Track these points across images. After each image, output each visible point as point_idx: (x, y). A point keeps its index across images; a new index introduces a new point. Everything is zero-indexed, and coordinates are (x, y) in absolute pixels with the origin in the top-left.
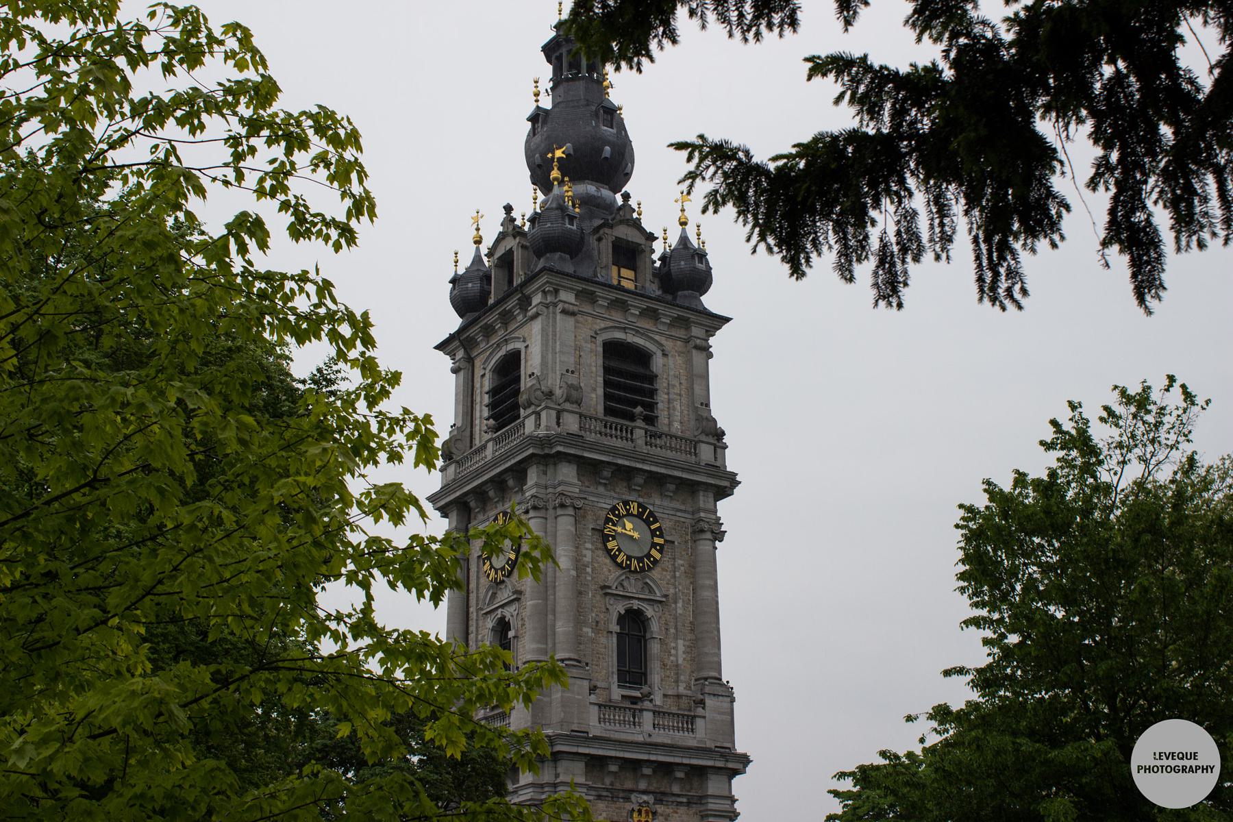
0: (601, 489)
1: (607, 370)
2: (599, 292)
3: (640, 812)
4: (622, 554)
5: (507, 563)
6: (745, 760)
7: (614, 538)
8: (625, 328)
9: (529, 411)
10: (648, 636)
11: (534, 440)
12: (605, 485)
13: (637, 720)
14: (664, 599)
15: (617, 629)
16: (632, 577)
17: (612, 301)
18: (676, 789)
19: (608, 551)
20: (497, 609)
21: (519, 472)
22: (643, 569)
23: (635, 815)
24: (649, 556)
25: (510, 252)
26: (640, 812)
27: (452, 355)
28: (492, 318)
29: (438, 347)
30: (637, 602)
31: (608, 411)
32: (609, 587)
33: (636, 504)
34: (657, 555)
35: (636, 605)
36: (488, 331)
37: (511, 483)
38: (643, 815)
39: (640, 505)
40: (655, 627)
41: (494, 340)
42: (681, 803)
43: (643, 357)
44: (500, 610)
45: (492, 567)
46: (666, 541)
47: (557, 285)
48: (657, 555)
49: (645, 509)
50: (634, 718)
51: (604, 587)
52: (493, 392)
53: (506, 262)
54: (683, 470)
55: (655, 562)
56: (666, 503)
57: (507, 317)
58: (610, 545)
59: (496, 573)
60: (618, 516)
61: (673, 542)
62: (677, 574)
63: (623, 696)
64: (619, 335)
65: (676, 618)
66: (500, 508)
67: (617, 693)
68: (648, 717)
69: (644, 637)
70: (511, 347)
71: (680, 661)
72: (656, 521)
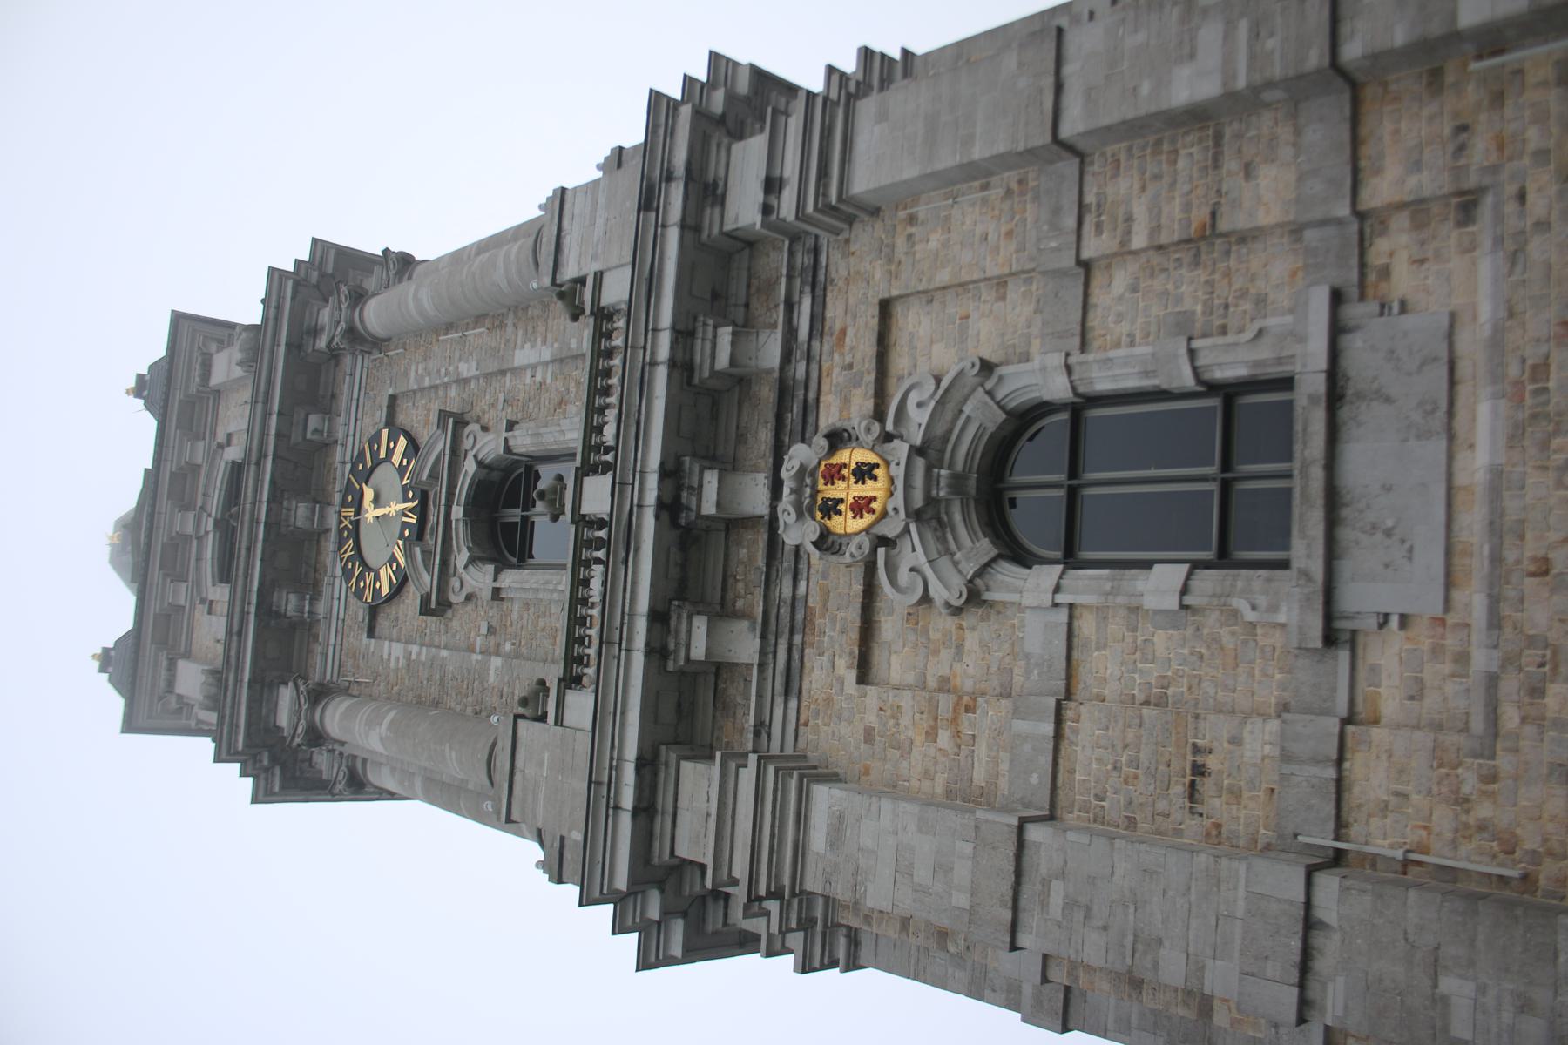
0: (321, 608)
3: (831, 508)
7: (377, 578)
12: (314, 600)
17: (166, 575)
18: (769, 351)
23: (837, 524)
26: (831, 508)
30: (455, 508)
35: (457, 512)
38: (838, 490)
39: (344, 504)
42: (817, 319)
54: (267, 414)
56: (340, 435)
58: (385, 590)
61: (393, 400)
62: (427, 383)
65: (488, 376)
71: (546, 355)
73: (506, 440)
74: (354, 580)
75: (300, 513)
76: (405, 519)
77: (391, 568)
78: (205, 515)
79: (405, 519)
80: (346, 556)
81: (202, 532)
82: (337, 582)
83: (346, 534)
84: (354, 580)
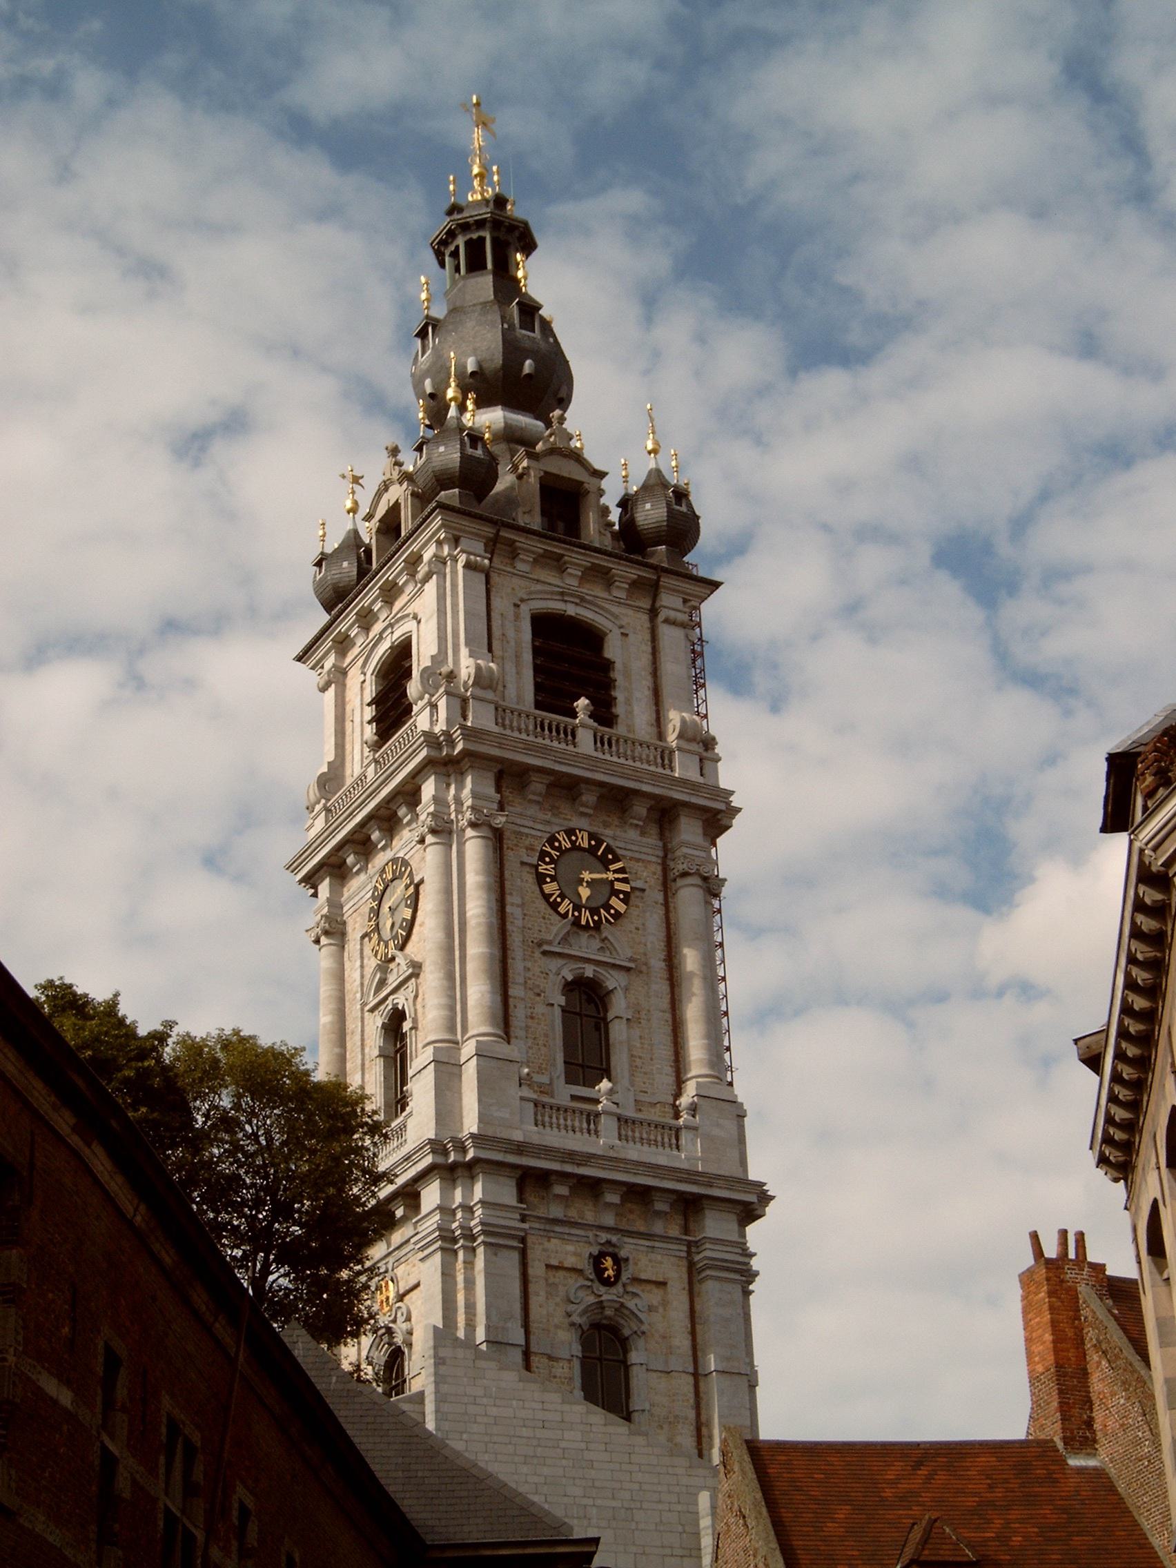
1: (536, 651)
2: (521, 540)
4: (567, 901)
5: (401, 927)
6: (765, 1198)
7: (553, 878)
8: (562, 594)
9: (421, 704)
10: (610, 1016)
11: (430, 739)
13: (592, 1126)
14: (632, 965)
15: (562, 1000)
16: (584, 936)
19: (546, 897)
20: (386, 998)
21: (409, 794)
22: (598, 924)
24: (608, 907)
25: (395, 509)
27: (317, 666)
28: (370, 597)
29: (300, 659)
31: (538, 705)
32: (550, 943)
33: (586, 835)
34: (621, 907)
35: (589, 971)
36: (366, 619)
37: (402, 811)
39: (592, 836)
40: (619, 1006)
41: (377, 628)
43: (592, 638)
44: (391, 998)
45: (380, 939)
46: (631, 888)
47: (460, 530)
48: (621, 907)
49: (600, 842)
50: (589, 1124)
51: (540, 945)
52: (377, 701)
53: (390, 527)
55: (618, 915)
57: (390, 593)
59: (387, 947)
60: (558, 849)
63: (574, 1098)
64: (556, 606)
66: (388, 855)
67: (564, 1093)
68: (608, 1125)
69: (605, 1019)
70: (399, 633)
72: (617, 859)
73: (621, 1018)
74: (549, 850)
75: (589, 798)
76: (583, 910)
77: (558, 896)
78: (578, 601)
79: (583, 910)
80: (561, 839)
81: (566, 598)
82: (548, 829)
83: (574, 838)
84: (549, 850)
